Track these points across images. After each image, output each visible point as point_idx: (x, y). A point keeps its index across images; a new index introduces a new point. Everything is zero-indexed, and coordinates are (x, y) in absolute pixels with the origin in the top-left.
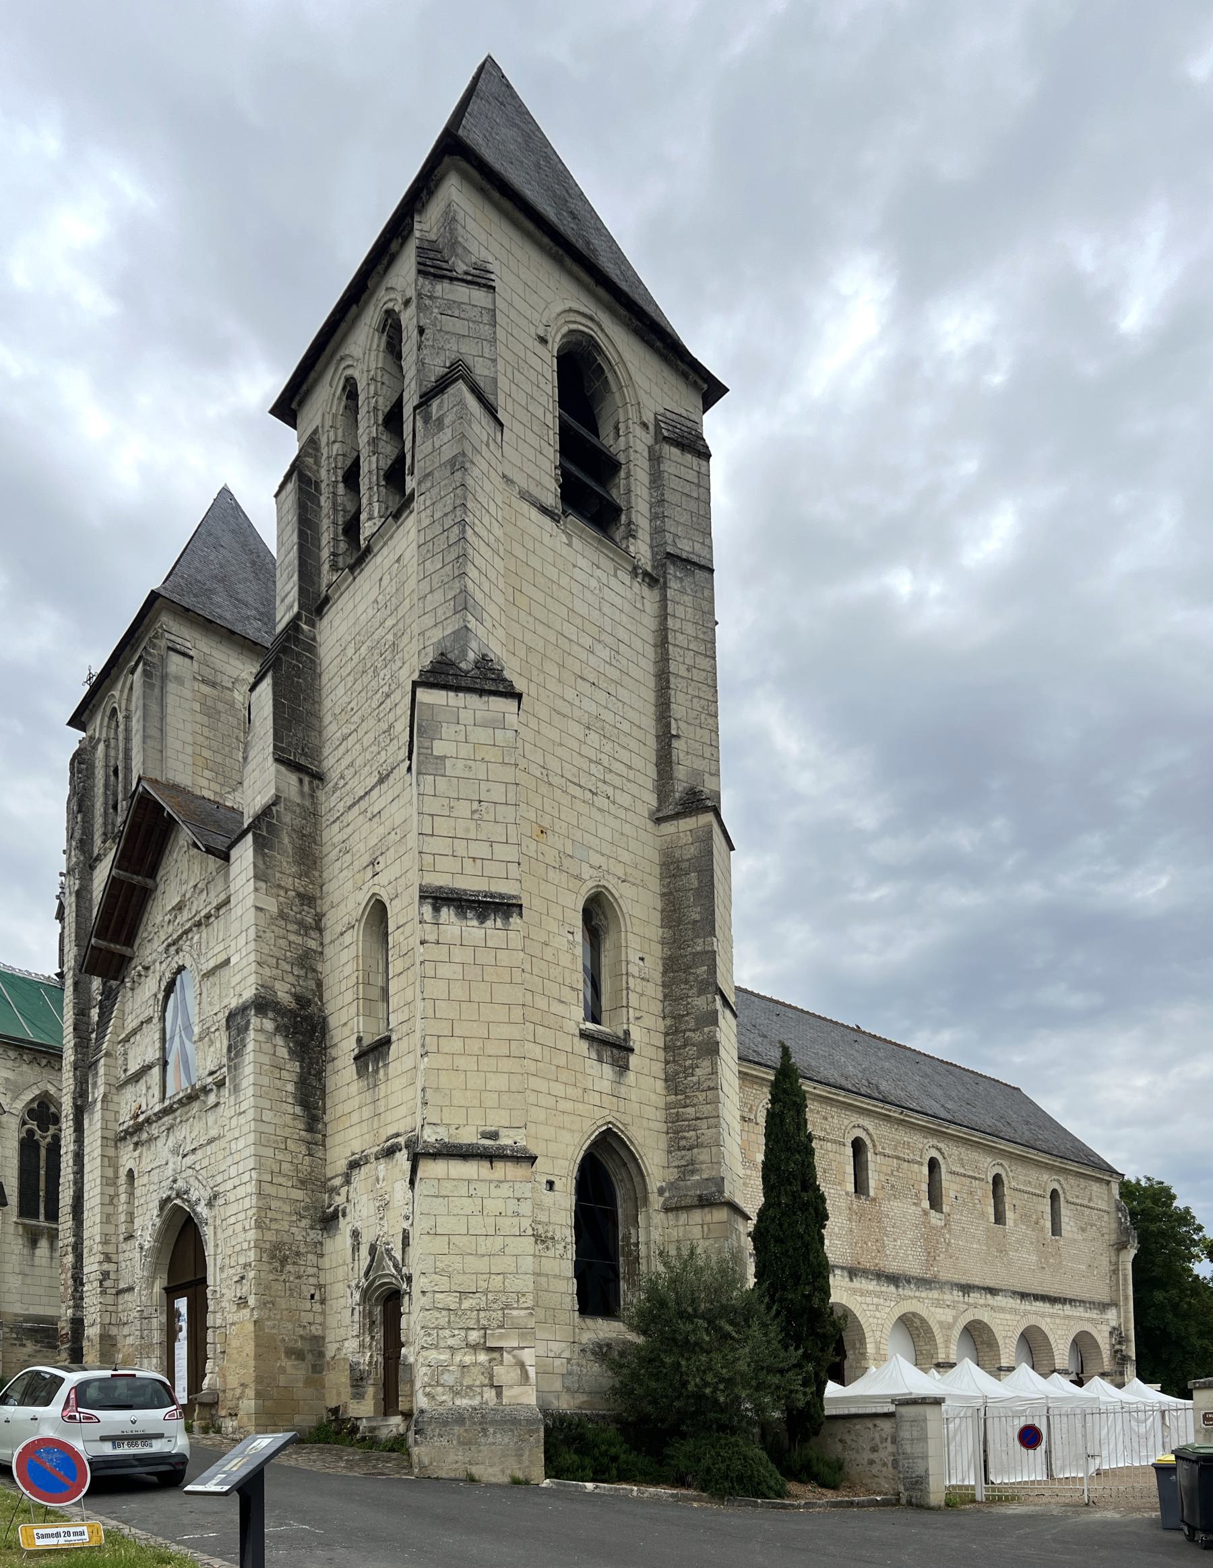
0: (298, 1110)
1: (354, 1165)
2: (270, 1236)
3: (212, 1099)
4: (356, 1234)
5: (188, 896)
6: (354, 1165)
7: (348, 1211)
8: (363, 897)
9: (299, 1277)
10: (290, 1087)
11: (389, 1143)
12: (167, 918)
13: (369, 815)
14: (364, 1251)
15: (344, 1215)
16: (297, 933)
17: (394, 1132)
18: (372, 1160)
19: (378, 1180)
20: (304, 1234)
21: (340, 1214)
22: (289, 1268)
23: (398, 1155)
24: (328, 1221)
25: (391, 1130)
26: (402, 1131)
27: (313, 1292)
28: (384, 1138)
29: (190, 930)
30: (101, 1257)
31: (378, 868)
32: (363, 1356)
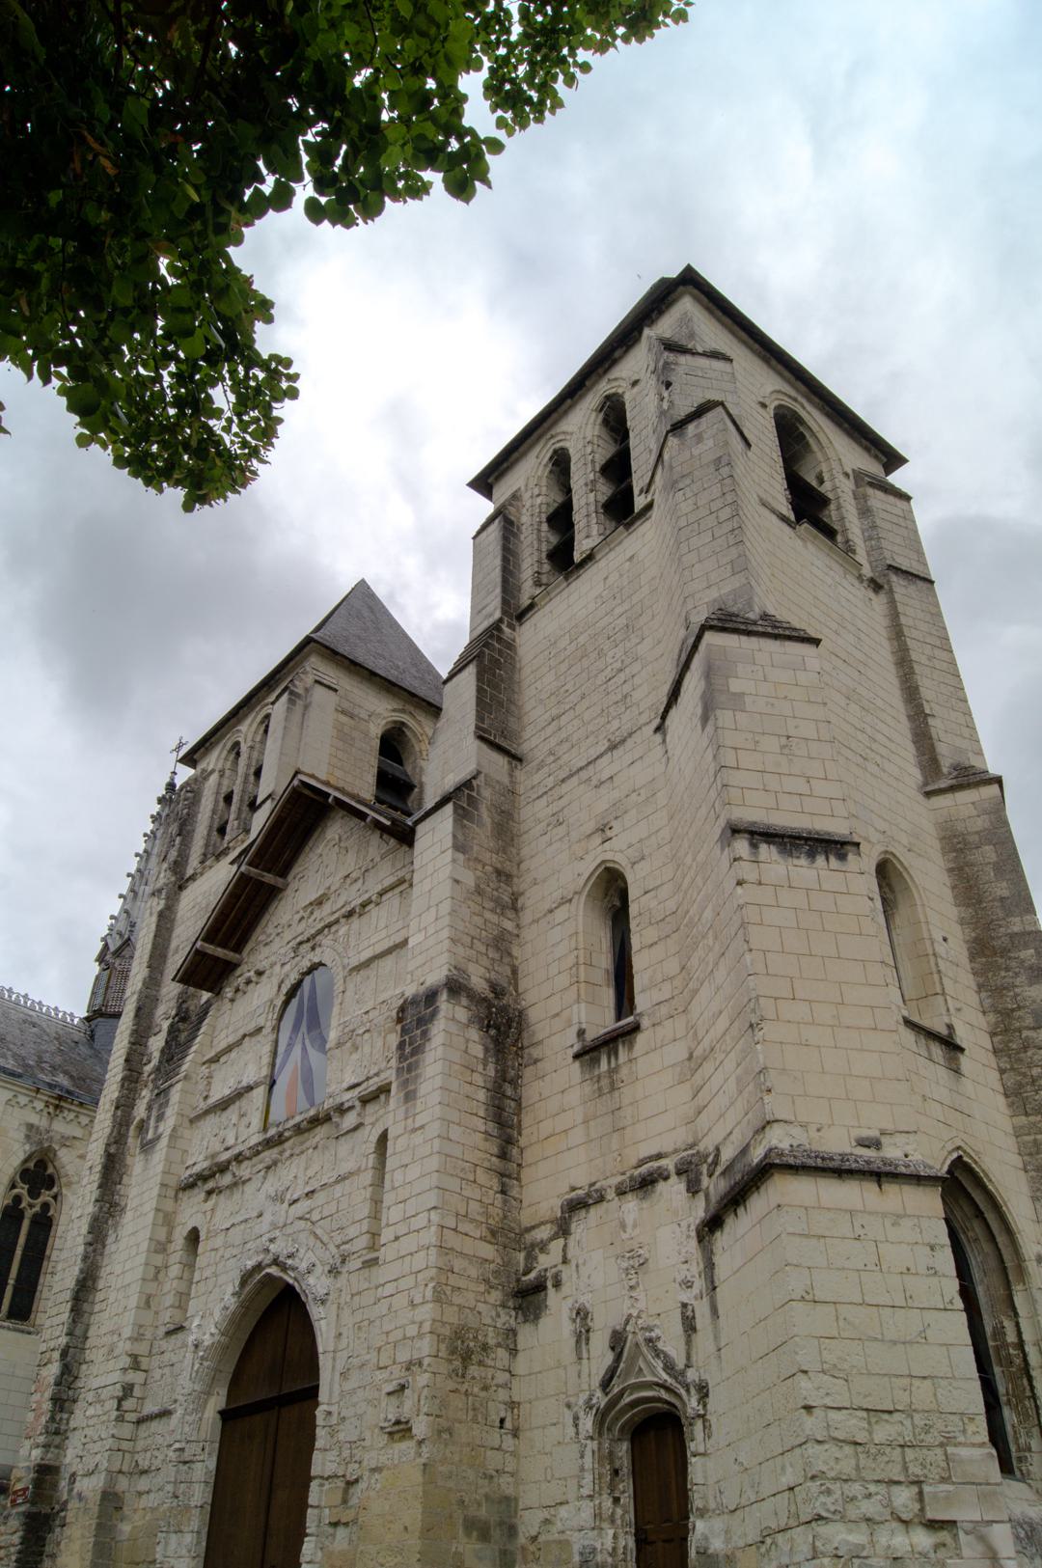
0: (492, 1127)
1: (577, 1206)
2: (452, 1316)
3: (350, 1120)
4: (582, 1314)
5: (333, 889)
6: (577, 1206)
7: (564, 1277)
8: (588, 866)
9: (485, 1388)
10: (482, 1095)
11: (644, 1169)
12: (298, 917)
13: (594, 782)
14: (600, 1342)
15: (557, 1285)
16: (493, 911)
17: (654, 1151)
18: (611, 1194)
19: (623, 1226)
20: (494, 1314)
21: (549, 1284)
22: (474, 1370)
23: (661, 1186)
24: (528, 1297)
25: (646, 1150)
26: (667, 1148)
27: (502, 1415)
28: (634, 1162)
29: (337, 921)
30: (126, 1361)
31: (609, 833)
32: (600, 1536)
